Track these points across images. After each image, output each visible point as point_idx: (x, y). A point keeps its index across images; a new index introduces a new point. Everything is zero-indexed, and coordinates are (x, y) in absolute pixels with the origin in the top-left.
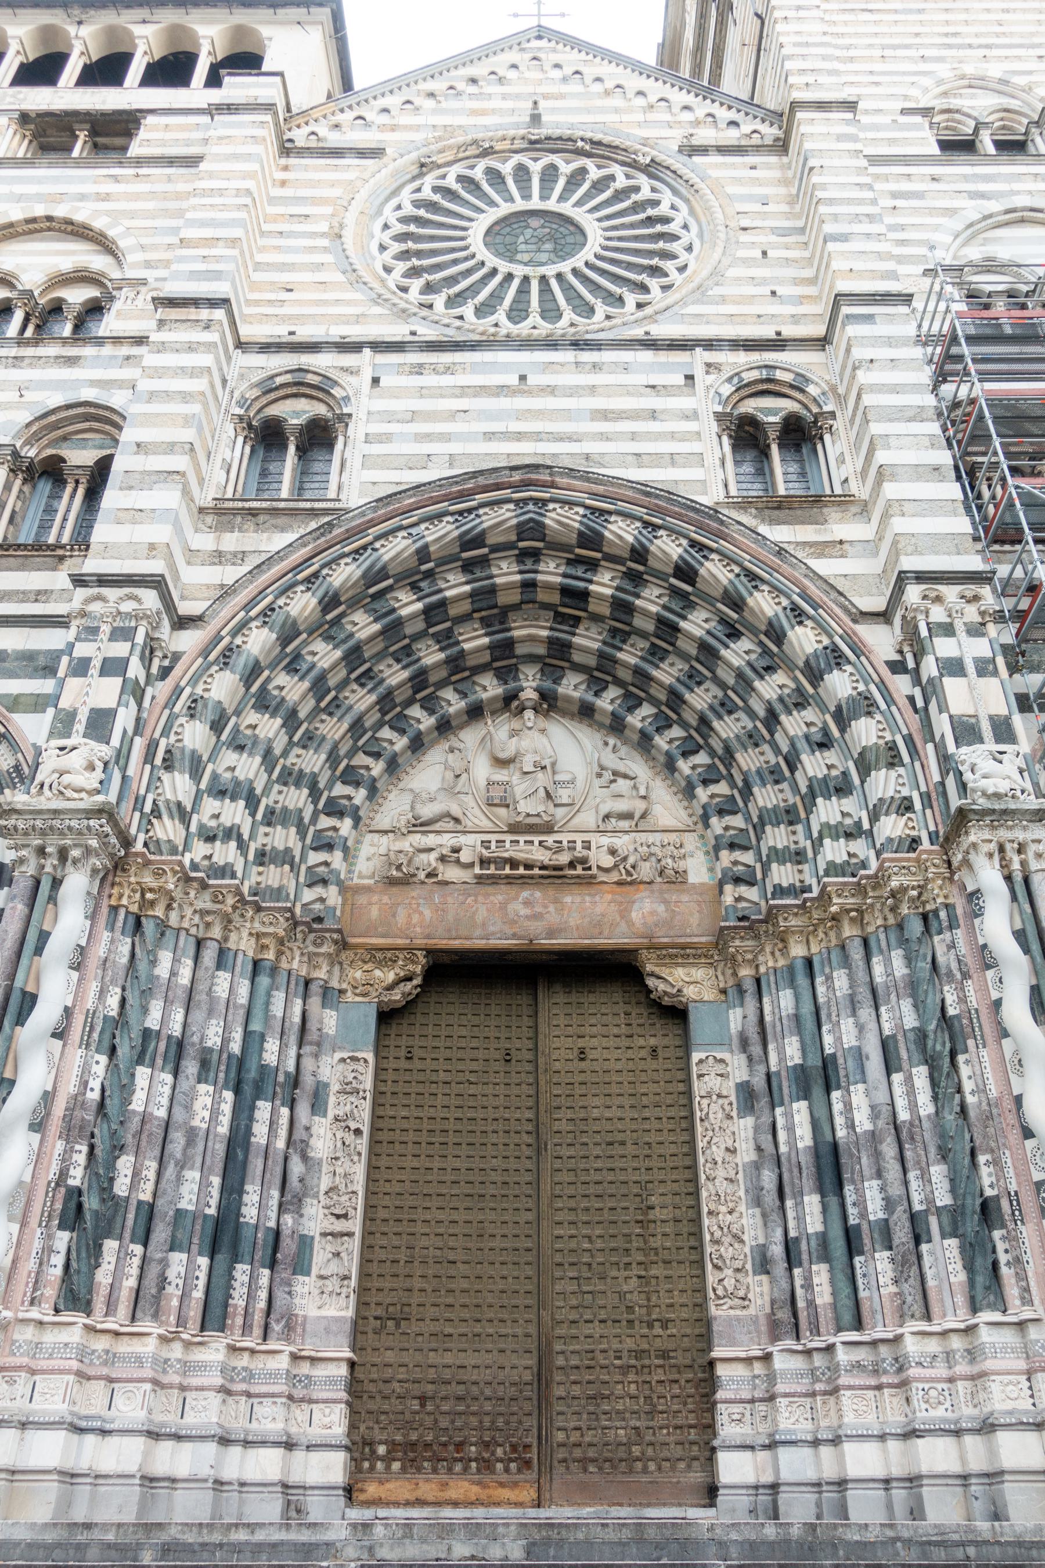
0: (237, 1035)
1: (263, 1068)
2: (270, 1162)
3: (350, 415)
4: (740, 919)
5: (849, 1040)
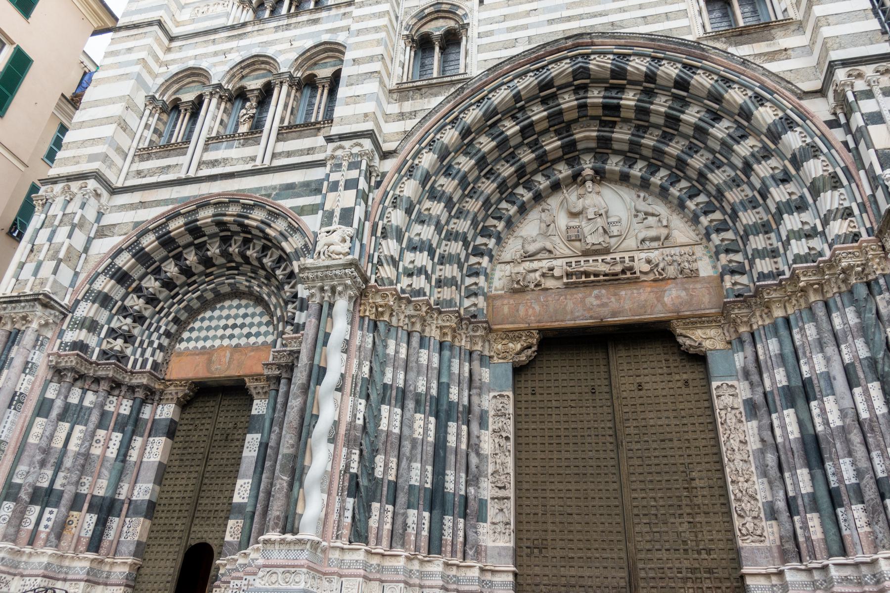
0: (434, 385)
1: (450, 404)
2: (459, 457)
3: (468, 24)
4: (737, 296)
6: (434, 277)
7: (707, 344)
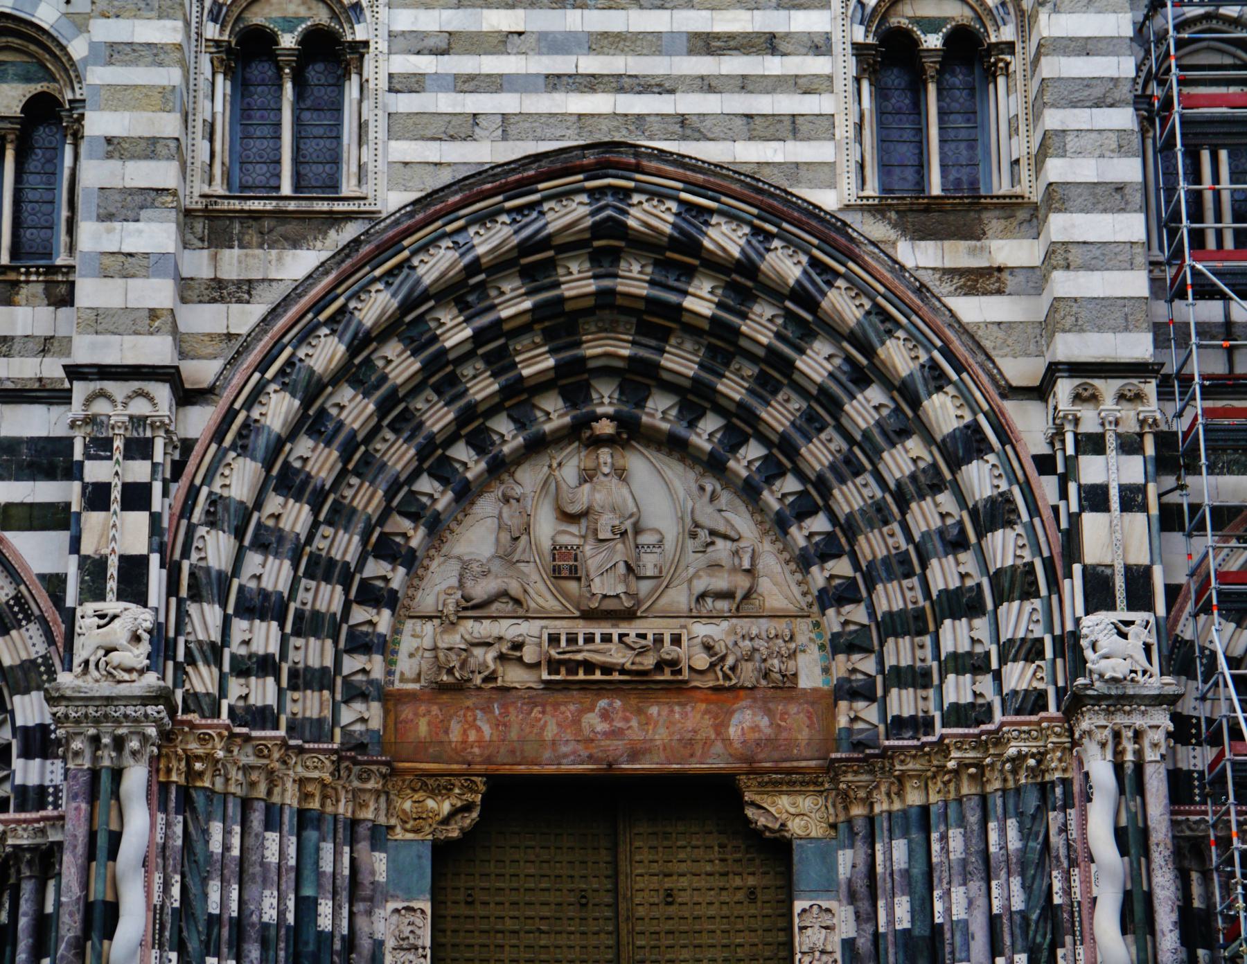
0: (291, 904)
3: (366, 44)
5: (959, 913)
7: (796, 827)
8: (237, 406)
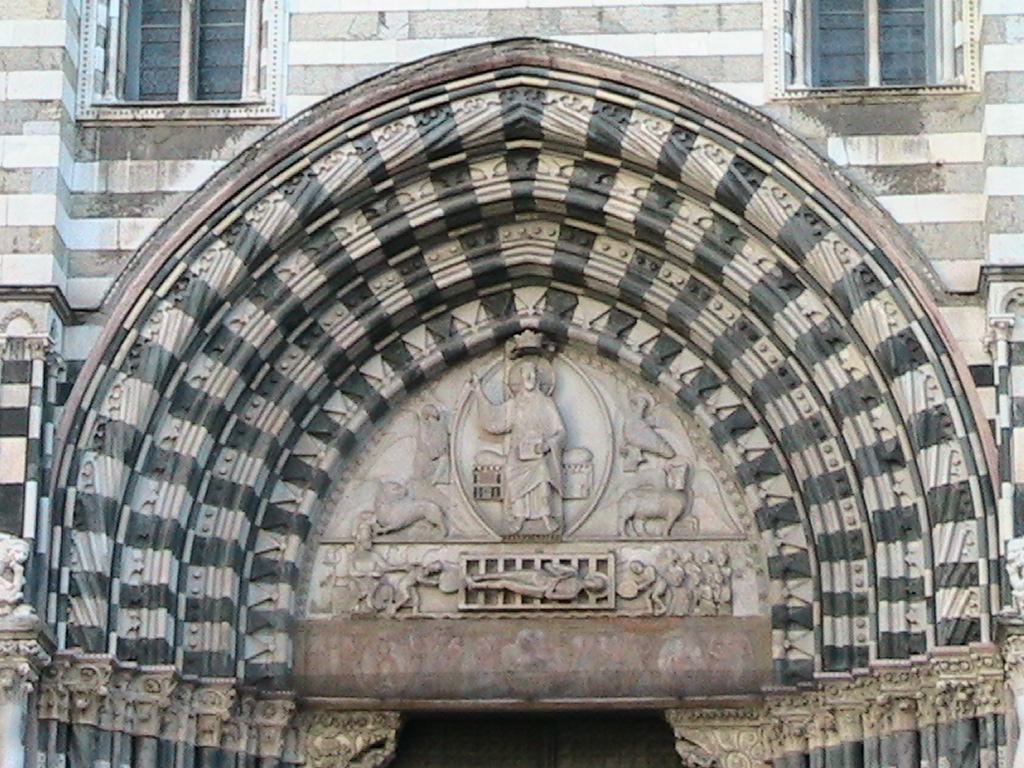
6: (182, 598)
8: (127, 325)
